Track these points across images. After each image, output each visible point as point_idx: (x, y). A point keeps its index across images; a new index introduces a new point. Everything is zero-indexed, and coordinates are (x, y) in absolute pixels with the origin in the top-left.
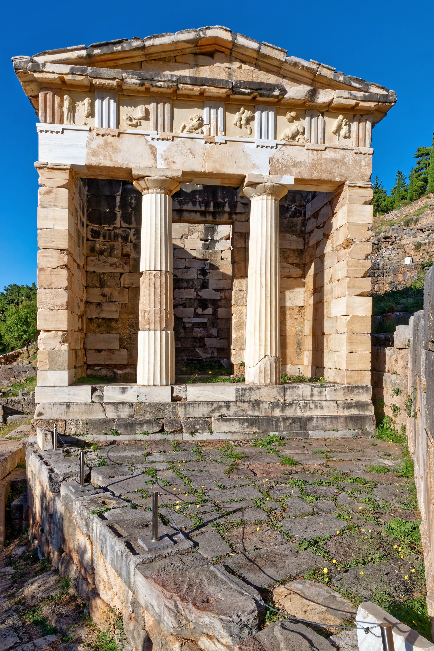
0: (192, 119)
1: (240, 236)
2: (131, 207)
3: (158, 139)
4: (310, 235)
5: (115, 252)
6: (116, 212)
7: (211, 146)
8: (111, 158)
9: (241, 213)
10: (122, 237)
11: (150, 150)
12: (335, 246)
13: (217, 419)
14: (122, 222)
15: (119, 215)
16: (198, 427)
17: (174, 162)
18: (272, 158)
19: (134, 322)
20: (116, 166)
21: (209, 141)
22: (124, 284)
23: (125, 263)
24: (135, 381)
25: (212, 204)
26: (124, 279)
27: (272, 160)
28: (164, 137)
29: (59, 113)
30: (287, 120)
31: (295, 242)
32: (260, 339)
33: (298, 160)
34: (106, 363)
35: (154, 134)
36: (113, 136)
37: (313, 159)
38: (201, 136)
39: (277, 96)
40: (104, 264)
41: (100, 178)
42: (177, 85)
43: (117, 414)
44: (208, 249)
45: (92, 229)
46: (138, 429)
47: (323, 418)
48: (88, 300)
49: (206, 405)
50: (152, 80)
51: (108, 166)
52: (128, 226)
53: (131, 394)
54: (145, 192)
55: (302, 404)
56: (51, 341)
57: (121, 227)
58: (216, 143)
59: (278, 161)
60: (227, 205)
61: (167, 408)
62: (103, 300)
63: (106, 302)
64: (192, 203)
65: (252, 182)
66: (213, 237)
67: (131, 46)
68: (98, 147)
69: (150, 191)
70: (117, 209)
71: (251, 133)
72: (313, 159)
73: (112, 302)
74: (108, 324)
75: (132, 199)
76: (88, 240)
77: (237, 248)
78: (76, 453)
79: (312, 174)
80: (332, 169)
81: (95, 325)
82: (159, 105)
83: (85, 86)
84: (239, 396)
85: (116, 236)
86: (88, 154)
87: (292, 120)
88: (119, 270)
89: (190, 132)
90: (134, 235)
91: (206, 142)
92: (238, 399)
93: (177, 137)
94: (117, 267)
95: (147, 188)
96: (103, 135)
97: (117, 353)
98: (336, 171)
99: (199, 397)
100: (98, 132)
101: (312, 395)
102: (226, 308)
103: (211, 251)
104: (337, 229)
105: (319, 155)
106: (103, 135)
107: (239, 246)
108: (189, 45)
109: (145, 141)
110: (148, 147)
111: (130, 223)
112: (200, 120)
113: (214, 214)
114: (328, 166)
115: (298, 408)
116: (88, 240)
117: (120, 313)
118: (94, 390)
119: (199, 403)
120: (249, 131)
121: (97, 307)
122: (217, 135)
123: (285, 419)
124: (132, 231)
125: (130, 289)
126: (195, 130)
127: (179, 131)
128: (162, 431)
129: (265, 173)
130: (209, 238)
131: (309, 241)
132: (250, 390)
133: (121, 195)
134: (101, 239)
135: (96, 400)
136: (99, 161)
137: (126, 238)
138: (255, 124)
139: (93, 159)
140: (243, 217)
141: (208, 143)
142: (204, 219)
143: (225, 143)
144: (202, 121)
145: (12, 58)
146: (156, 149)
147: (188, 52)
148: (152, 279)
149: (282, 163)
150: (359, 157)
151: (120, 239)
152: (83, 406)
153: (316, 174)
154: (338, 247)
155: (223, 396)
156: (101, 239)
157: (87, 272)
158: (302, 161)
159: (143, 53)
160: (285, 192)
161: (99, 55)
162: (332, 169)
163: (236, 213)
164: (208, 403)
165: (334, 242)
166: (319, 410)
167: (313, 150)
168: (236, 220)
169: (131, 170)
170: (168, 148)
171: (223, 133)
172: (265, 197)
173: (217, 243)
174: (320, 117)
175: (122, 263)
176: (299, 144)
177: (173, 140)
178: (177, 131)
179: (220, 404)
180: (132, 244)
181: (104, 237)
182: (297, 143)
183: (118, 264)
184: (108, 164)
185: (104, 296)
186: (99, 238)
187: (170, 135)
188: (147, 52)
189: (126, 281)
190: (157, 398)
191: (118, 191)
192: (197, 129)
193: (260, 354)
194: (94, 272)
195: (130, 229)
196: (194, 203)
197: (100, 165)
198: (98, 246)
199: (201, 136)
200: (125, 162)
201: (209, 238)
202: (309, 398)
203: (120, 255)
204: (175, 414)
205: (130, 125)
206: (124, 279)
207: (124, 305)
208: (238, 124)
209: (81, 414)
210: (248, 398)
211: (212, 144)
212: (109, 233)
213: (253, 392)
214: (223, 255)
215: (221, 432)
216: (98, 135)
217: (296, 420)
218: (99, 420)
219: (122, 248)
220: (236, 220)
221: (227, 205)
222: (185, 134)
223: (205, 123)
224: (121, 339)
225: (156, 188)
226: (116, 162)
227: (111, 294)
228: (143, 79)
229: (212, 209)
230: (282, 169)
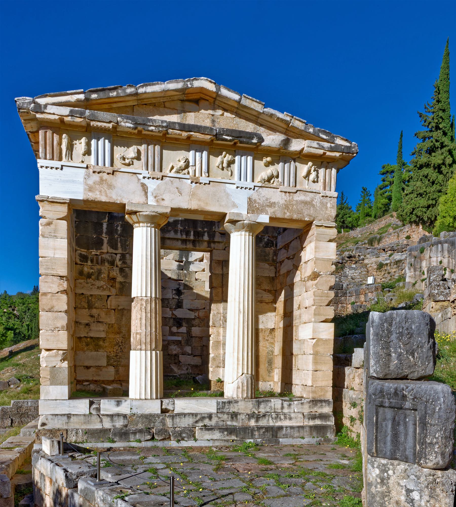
0: (179, 161)
3: (149, 178)
7: (196, 186)
8: (106, 193)
11: (141, 188)
12: (303, 277)
13: (200, 429)
16: (184, 435)
20: (111, 201)
21: (195, 181)
24: (127, 395)
26: (111, 301)
28: (154, 176)
29: (58, 151)
30: (263, 164)
31: (269, 271)
32: (238, 359)
34: (95, 379)
38: (187, 176)
42: (167, 130)
43: (113, 424)
46: (132, 437)
48: (77, 320)
50: (144, 124)
51: (104, 201)
56: (53, 359)
58: (200, 183)
61: (157, 418)
65: (233, 219)
67: (125, 92)
71: (232, 175)
73: (100, 322)
74: (95, 343)
78: (80, 457)
82: (150, 147)
87: (268, 165)
89: (177, 172)
91: (192, 183)
93: (166, 176)
97: (104, 369)
104: (305, 263)
108: (178, 93)
109: (137, 179)
110: (140, 185)
112: (187, 161)
118: (91, 403)
120: (230, 173)
121: (85, 327)
122: (201, 176)
126: (182, 170)
127: (168, 171)
128: (153, 439)
129: (244, 212)
135: (94, 412)
136: (95, 197)
138: (235, 167)
141: (193, 183)
143: (209, 184)
144: (189, 162)
145: (16, 99)
146: (147, 187)
147: (176, 99)
152: (82, 417)
154: (306, 279)
159: (135, 98)
160: (261, 229)
161: (96, 100)
165: (303, 274)
170: (158, 186)
171: (207, 174)
174: (292, 162)
176: (274, 187)
177: (162, 179)
178: (166, 171)
184: (104, 199)
187: (160, 175)
188: (139, 97)
189: (113, 302)
190: (148, 411)
192: (184, 169)
199: (187, 176)
200: (119, 198)
204: (164, 424)
205: (123, 164)
208: (220, 167)
209: (80, 424)
211: (197, 184)
215: (204, 439)
218: (97, 430)
222: (173, 174)
223: (191, 164)
226: (111, 197)
228: (136, 124)
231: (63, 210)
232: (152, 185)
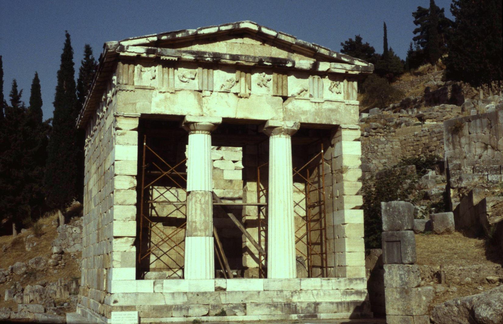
17: (215, 111)
20: (173, 114)
33: (304, 109)
36: (172, 93)
39: (290, 67)
49: (241, 293)
51: (168, 113)
53: (182, 286)
68: (160, 100)
69: (197, 132)
79: (315, 119)
83: (151, 58)
92: (265, 289)
95: (195, 130)
96: (164, 92)
98: (333, 117)
100: (161, 90)
106: (164, 92)
119: (236, 292)
149: (293, 112)
150: (349, 107)
153: (318, 120)
158: (308, 110)
162: (330, 116)
164: (243, 292)
167: (315, 103)
172: (282, 136)
179: (252, 293)
182: (303, 98)
184: (168, 112)
197: (162, 113)
216: (160, 92)
225: (202, 130)
231: (135, 123)
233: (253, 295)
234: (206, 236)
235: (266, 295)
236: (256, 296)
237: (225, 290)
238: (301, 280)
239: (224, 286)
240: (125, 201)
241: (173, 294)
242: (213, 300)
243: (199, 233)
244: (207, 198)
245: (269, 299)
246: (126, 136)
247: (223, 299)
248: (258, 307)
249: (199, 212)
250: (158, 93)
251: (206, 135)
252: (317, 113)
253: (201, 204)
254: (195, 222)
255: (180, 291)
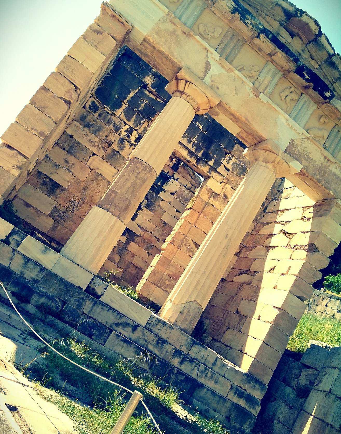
1: (209, 191)
2: (137, 108)
4: (264, 226)
5: (101, 133)
6: (123, 103)
9: (220, 174)
10: (114, 125)
14: (123, 114)
15: (124, 107)
17: (218, 88)
18: (293, 141)
19: (78, 201)
22: (90, 164)
23: (103, 148)
25: (202, 152)
27: (292, 143)
33: (311, 156)
35: (216, 55)
36: (183, 32)
37: (322, 164)
40: (84, 136)
41: (143, 58)
44: (153, 191)
45: (94, 102)
47: (214, 393)
49: (115, 314)
52: (125, 120)
54: (178, 94)
55: (202, 367)
57: (118, 117)
59: (296, 146)
60: (213, 160)
62: (64, 164)
63: (64, 168)
64: (188, 140)
66: (163, 184)
68: (165, 30)
69: (184, 96)
70: (125, 101)
72: (322, 164)
75: (143, 102)
76: (84, 107)
77: (201, 198)
79: (315, 174)
80: (331, 181)
81: (41, 181)
84: (150, 324)
85: (109, 122)
86: (153, 29)
88: (94, 150)
90: (126, 131)
94: (94, 146)
99: (113, 302)
101: (214, 364)
102: (138, 245)
103: (154, 194)
105: (328, 164)
107: (203, 198)
110: (205, 62)
111: (129, 120)
113: (199, 160)
114: (330, 177)
115: (196, 369)
116: (84, 107)
117: (71, 185)
119: (110, 308)
123: (180, 373)
124: (126, 127)
125: (93, 171)
130: (159, 184)
131: (260, 230)
132: (163, 325)
133: (136, 94)
134: (97, 114)
137: (117, 129)
139: (155, 36)
140: (219, 178)
142: (189, 158)
148: (138, 168)
149: (298, 150)
151: (111, 126)
155: (136, 316)
156: (97, 114)
157: (65, 131)
163: (216, 171)
164: (119, 313)
166: (213, 382)
167: (325, 157)
168: (212, 177)
169: (179, 69)
173: (163, 192)
175: (100, 146)
179: (129, 321)
180: (119, 137)
181: (100, 115)
183: (96, 144)
185: (66, 161)
186: (95, 112)
191: (136, 89)
193: (190, 296)
194: (71, 136)
195: (125, 124)
196: (189, 141)
198: (90, 117)
201: (159, 184)
202: (210, 366)
203: (103, 138)
206: (94, 160)
207: (78, 181)
208: (283, 98)
210: (158, 331)
212: (105, 115)
213: (165, 328)
214: (162, 203)
217: (189, 379)
219: (109, 135)
220: (212, 177)
221: (213, 160)
224: (55, 208)
227: (73, 164)
229: (200, 155)
230: (295, 154)
232: (215, 69)
233: (128, 324)
234: (118, 218)
235: (144, 335)
236: (130, 329)
237: (98, 297)
238: (194, 343)
239: (99, 291)
240: (45, 107)
241: (28, 260)
242: (75, 300)
243: (112, 209)
244: (148, 176)
245: (144, 342)
246: (99, 35)
247: (87, 306)
248: (125, 345)
249: (129, 184)
250: (168, 20)
251: (192, 108)
252: (320, 169)
253: (136, 177)
254: (116, 194)
255: (40, 262)
